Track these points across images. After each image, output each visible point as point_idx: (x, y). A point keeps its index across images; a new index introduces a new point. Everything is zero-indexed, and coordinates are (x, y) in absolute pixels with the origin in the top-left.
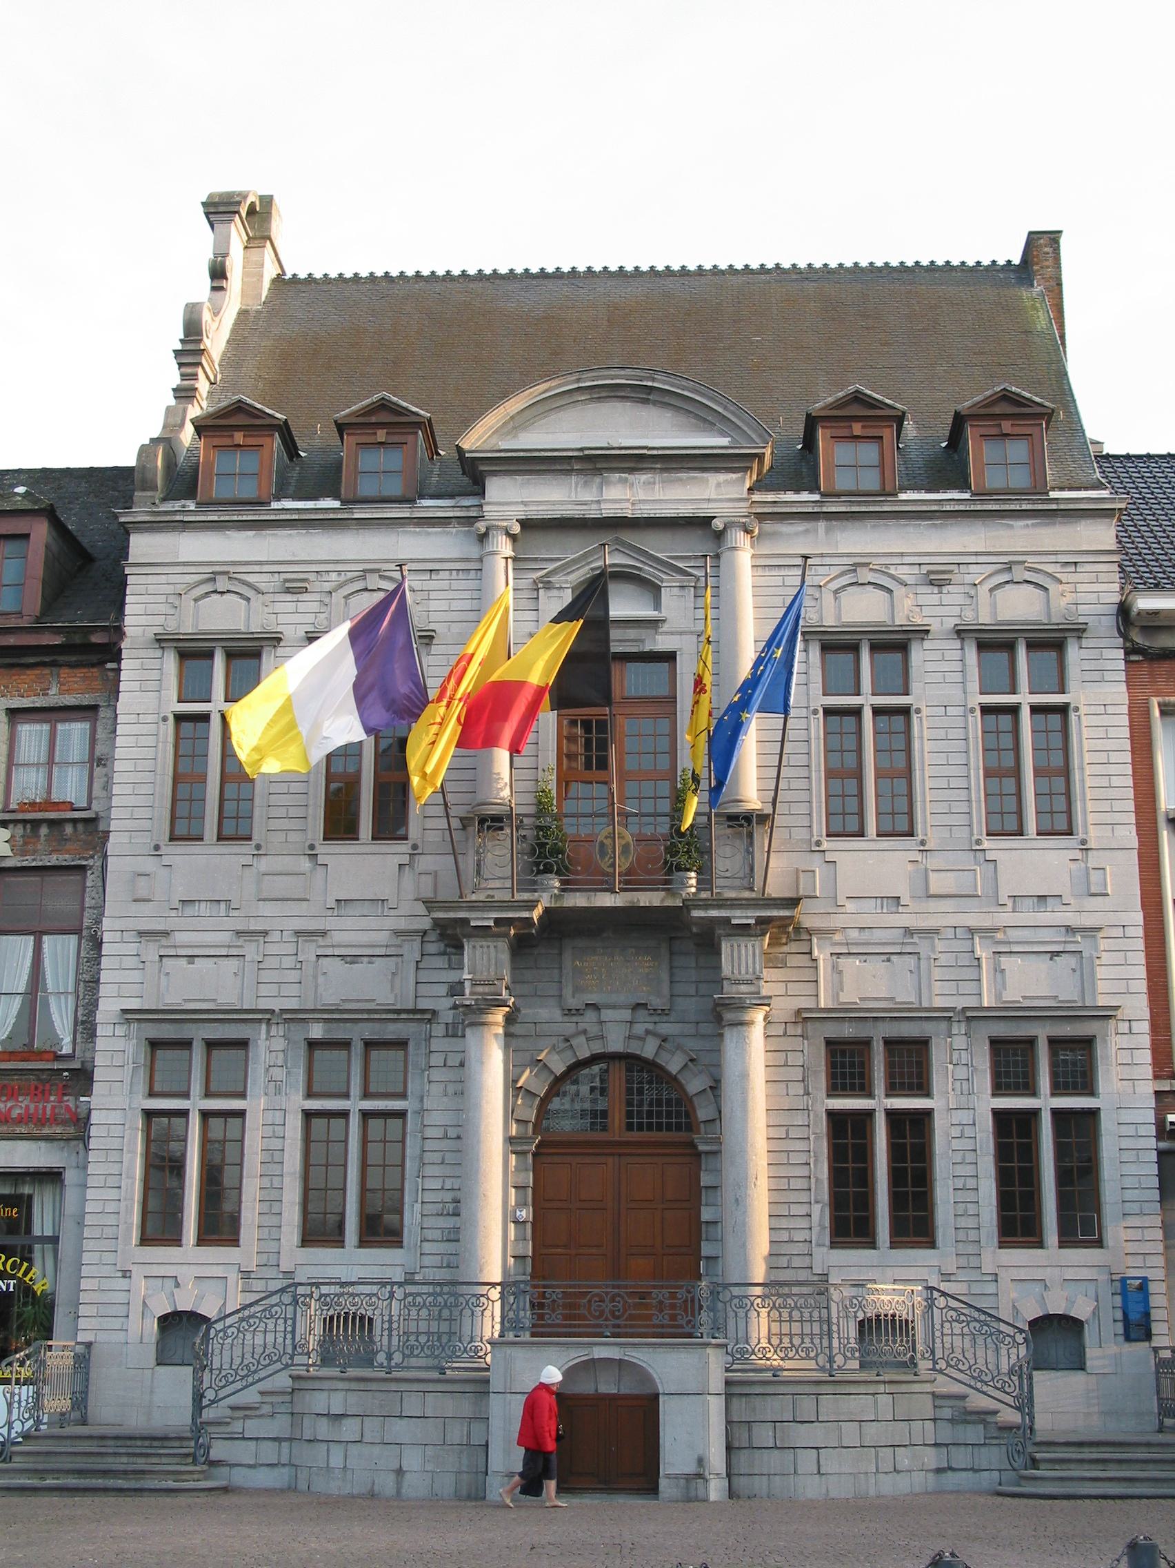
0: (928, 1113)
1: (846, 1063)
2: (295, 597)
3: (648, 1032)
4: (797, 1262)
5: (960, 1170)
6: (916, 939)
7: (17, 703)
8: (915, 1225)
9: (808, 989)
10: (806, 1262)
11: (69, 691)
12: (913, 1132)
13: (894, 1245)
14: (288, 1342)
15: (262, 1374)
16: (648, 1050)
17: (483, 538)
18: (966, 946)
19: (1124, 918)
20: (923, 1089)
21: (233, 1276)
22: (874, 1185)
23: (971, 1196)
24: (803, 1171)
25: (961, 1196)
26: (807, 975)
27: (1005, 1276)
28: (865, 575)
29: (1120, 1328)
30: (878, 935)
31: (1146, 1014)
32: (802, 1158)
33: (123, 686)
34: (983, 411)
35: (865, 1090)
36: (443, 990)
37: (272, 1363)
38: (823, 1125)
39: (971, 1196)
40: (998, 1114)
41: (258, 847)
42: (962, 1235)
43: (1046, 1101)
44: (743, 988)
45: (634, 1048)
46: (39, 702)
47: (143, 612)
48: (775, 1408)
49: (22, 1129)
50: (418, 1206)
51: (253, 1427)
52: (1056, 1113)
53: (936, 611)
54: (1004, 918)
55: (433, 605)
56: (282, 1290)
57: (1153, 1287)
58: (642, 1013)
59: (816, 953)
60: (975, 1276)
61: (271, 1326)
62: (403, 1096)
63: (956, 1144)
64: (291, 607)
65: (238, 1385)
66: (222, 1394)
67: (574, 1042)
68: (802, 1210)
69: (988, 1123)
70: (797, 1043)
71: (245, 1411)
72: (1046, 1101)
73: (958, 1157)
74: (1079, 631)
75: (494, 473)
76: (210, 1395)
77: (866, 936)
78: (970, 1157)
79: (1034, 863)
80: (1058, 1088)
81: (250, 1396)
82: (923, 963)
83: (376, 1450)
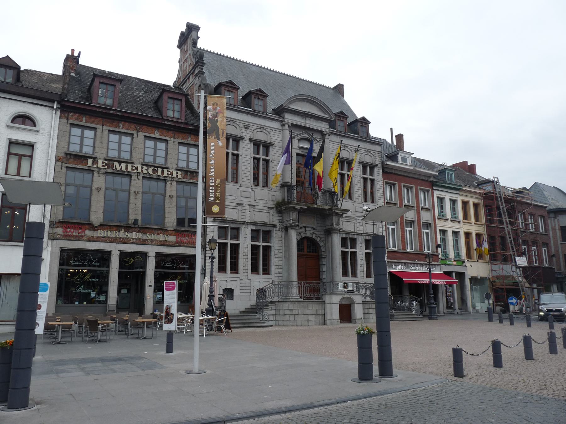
7: (180, 141)
17: (283, 125)
20: (355, 248)
21: (238, 279)
46: (186, 142)
72: (229, 241)
74: (376, 166)
75: (286, 112)
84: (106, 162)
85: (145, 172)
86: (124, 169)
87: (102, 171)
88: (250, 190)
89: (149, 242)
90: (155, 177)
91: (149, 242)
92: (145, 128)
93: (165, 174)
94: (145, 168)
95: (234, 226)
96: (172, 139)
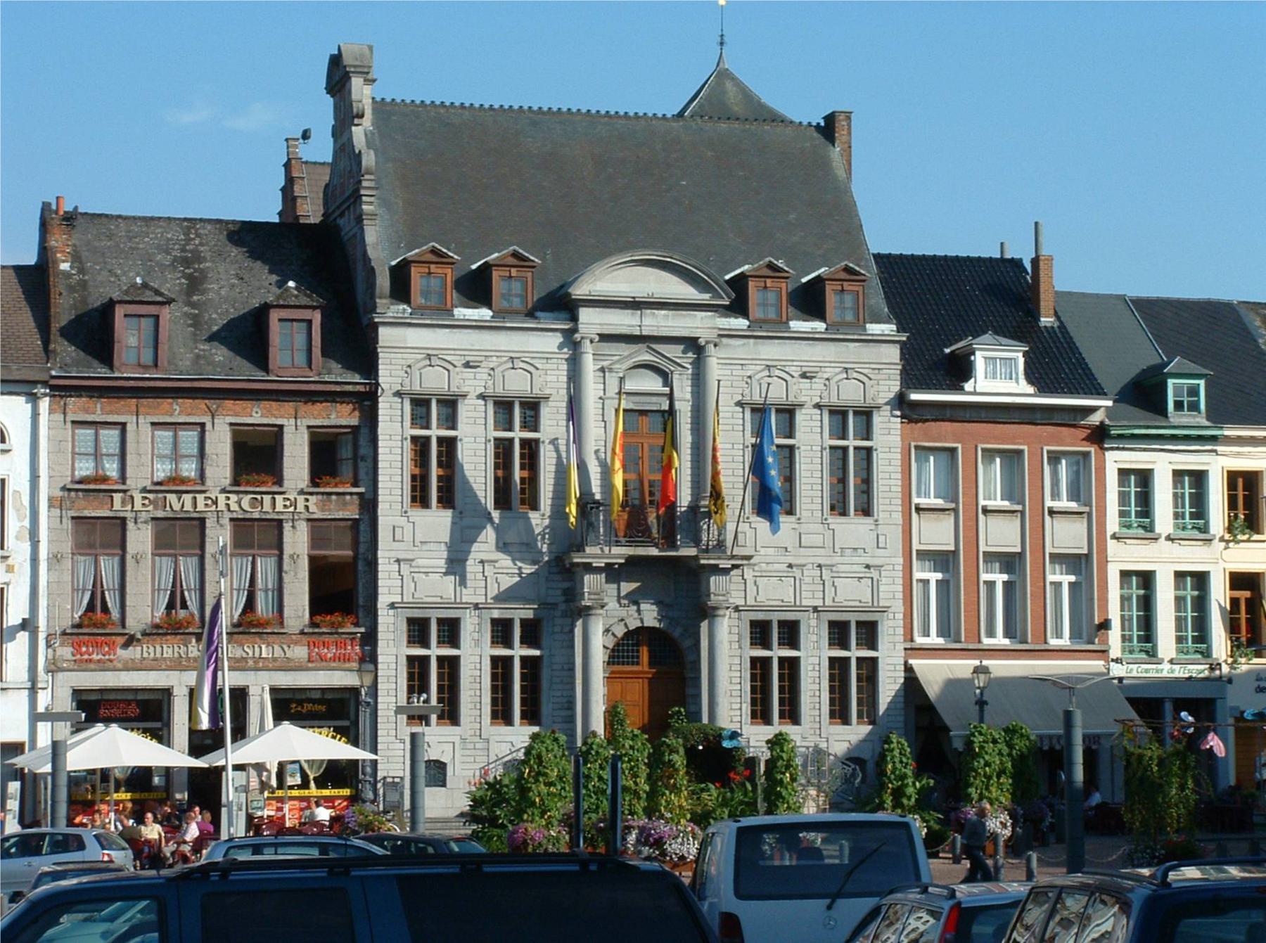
1: (760, 632)
12: (791, 667)
19: (894, 560)
30: (777, 567)
36: (559, 592)
40: (832, 660)
47: (389, 375)
52: (858, 659)
53: (807, 393)
54: (837, 559)
55: (549, 378)
77: (770, 567)
79: (853, 529)
84: (151, 496)
85: (234, 507)
86: (188, 507)
87: (144, 516)
89: (251, 663)
90: (256, 516)
91: (251, 663)
92: (229, 403)
93: (279, 508)
94: (234, 497)
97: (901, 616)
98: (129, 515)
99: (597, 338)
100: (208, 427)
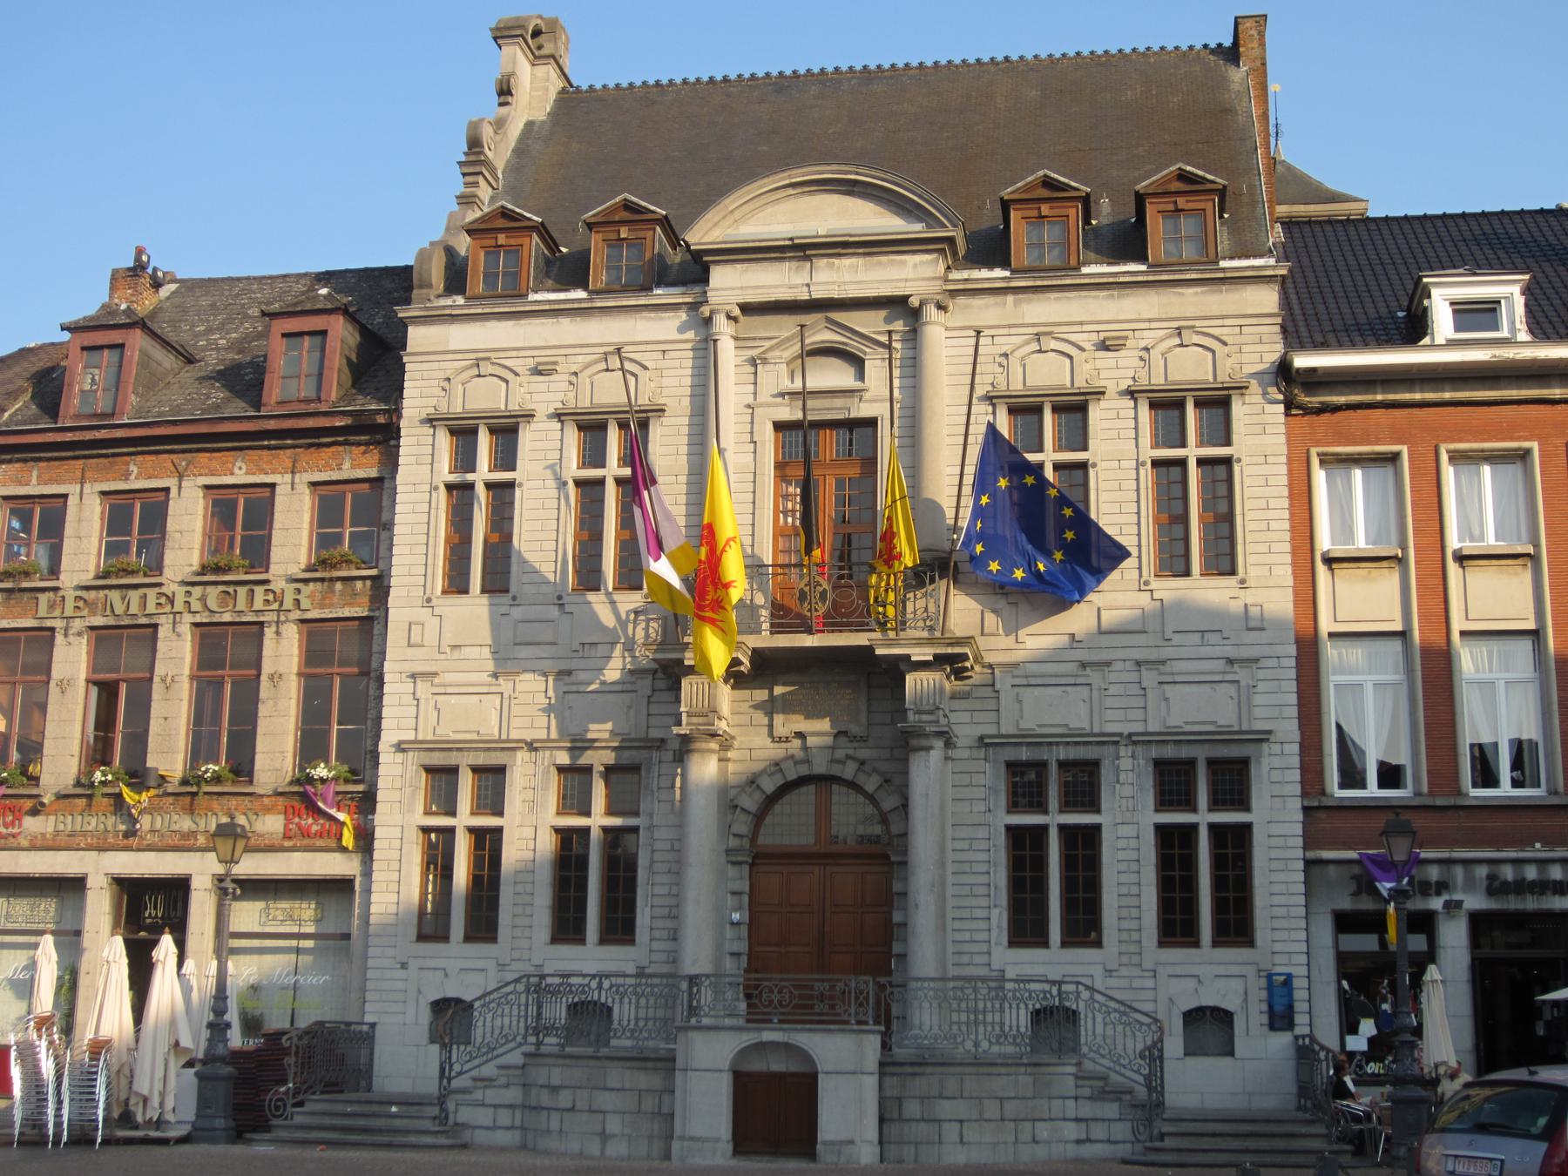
0: (1097, 828)
1: (1025, 783)
2: (546, 378)
3: (848, 757)
4: (977, 959)
5: (1123, 878)
6: (1236, 667)
8: (1084, 925)
9: (992, 716)
10: (984, 959)
11: (359, 466)
12: (1084, 846)
13: (1065, 944)
14: (522, 1024)
15: (500, 1051)
16: (849, 771)
18: (1134, 677)
19: (1280, 650)
22: (1051, 887)
23: (1134, 901)
24: (983, 879)
25: (1124, 901)
26: (992, 704)
27: (1162, 971)
28: (486, 368)
29: (1265, 1019)
31: (1296, 736)
32: (984, 868)
33: (401, 460)
34: (483, 226)
35: (1190, 805)
37: (508, 1042)
38: (1001, 839)
39: (1134, 901)
40: (1160, 828)
41: (514, 598)
42: (1124, 936)
43: (1204, 817)
44: (925, 717)
45: (836, 770)
46: (335, 476)
47: (420, 394)
48: (920, 1085)
49: (320, 843)
50: (648, 910)
51: (492, 1096)
54: (1168, 652)
55: (666, 382)
56: (517, 981)
57: (1296, 983)
58: (843, 739)
59: (998, 686)
60: (1136, 972)
61: (507, 1011)
62: (636, 814)
63: (1121, 855)
64: (543, 387)
65: (476, 1062)
66: (466, 1067)
67: (783, 766)
68: (984, 913)
69: (1150, 837)
70: (981, 765)
71: (487, 1082)
73: (1123, 867)
76: (457, 1068)
78: (1134, 867)
80: (1216, 804)
81: (489, 1070)
82: (1095, 693)
83: (585, 1116)
85: (196, 606)
88: (554, 612)
91: (201, 840)
92: (203, 457)
95: (482, 759)
96: (288, 477)
97: (1296, 748)
98: (58, 624)
99: (737, 312)
100: (174, 492)
